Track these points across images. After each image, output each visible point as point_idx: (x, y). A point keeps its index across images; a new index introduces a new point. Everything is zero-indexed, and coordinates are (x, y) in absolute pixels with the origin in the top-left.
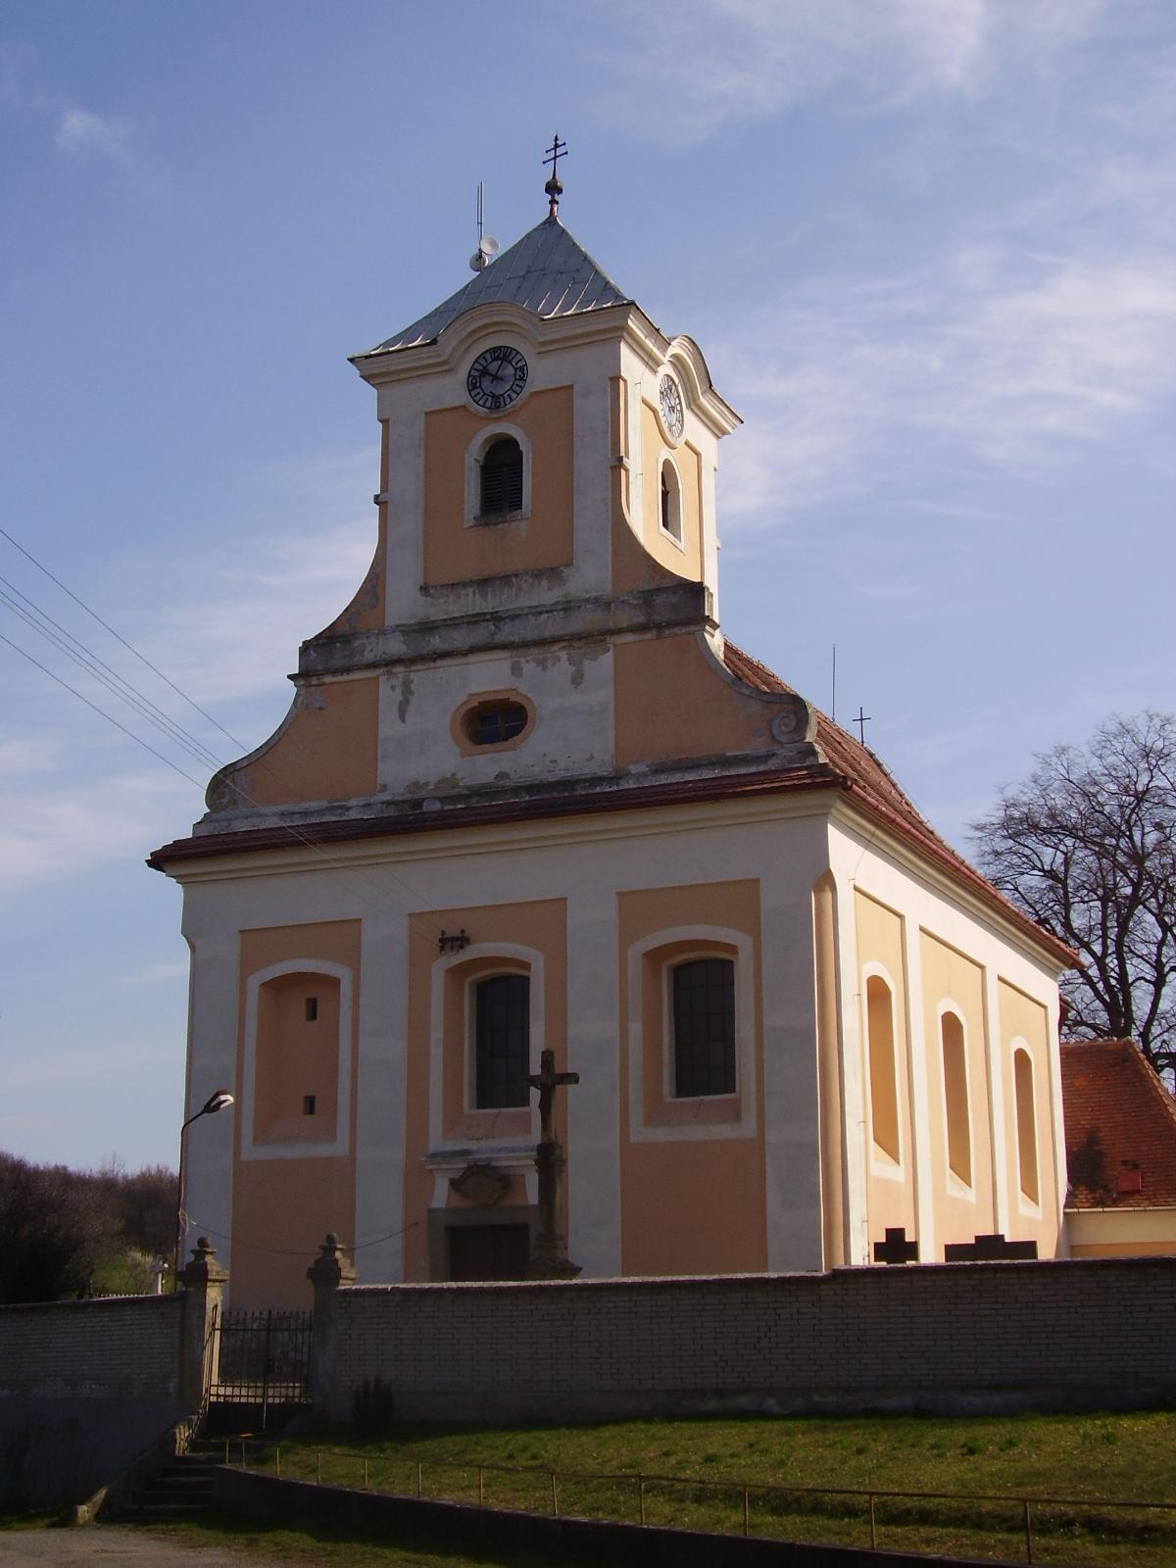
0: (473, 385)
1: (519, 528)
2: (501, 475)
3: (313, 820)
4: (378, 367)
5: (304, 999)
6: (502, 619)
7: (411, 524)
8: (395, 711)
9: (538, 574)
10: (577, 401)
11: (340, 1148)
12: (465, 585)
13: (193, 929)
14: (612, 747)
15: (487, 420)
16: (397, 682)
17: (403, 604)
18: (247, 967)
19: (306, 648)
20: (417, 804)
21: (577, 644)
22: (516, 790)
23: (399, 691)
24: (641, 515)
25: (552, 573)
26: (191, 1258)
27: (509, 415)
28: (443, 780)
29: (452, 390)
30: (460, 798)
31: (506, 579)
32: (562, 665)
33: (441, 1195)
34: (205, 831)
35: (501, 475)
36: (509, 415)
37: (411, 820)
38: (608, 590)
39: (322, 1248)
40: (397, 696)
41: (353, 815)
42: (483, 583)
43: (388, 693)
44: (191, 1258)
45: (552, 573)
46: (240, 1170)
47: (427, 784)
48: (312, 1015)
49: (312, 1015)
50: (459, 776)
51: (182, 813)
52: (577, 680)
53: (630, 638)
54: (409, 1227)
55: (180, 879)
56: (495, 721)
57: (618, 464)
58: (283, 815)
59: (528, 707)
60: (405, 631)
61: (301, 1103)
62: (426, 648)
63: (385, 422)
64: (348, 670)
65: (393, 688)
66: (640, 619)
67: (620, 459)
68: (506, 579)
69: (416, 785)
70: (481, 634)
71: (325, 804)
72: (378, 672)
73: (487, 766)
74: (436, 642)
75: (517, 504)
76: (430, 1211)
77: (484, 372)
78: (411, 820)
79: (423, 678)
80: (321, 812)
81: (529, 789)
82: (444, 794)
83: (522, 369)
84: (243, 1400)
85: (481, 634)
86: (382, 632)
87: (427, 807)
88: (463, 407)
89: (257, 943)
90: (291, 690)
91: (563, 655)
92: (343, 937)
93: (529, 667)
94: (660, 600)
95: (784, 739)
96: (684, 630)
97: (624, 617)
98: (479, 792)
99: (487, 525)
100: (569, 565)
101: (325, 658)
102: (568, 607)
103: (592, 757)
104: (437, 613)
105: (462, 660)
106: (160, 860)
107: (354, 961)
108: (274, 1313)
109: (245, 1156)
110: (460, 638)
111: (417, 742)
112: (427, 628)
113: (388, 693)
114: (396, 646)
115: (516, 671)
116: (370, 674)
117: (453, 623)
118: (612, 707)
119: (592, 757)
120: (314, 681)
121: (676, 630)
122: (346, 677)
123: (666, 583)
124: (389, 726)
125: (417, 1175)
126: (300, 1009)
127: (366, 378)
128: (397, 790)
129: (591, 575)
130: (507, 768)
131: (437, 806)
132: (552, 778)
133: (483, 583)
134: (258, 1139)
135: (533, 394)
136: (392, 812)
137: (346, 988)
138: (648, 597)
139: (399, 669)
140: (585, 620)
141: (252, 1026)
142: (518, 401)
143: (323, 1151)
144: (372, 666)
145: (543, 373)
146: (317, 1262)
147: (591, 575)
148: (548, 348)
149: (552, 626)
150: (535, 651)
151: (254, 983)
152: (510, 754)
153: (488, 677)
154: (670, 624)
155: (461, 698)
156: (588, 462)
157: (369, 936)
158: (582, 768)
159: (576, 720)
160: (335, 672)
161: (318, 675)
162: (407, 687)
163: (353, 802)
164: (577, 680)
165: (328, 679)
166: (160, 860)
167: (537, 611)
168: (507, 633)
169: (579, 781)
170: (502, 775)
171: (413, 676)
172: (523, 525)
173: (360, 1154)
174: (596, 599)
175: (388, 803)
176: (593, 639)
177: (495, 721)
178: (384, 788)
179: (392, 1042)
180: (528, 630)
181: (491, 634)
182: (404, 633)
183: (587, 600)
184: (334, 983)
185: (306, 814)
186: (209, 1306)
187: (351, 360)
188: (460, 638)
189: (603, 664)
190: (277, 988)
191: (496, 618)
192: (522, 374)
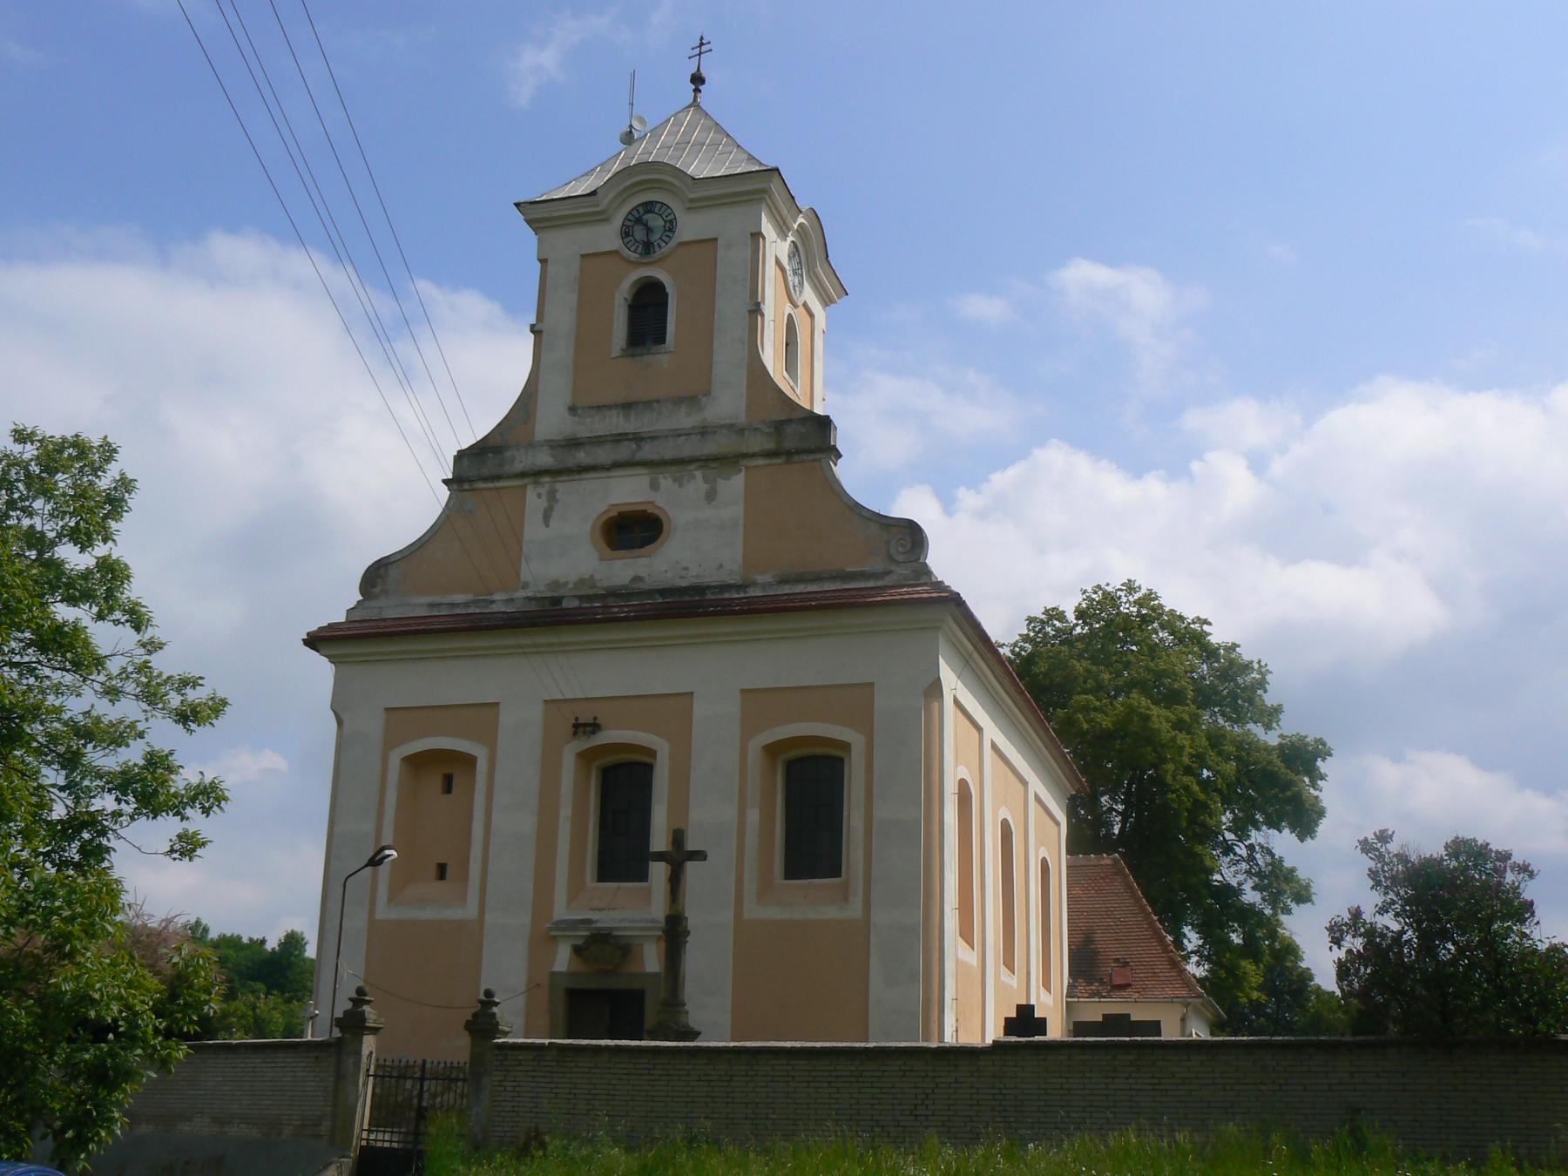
0: (626, 233)
1: (662, 360)
2: (648, 312)
3: (459, 611)
4: (539, 213)
5: (443, 772)
6: (643, 439)
7: (563, 352)
8: (540, 516)
9: (678, 401)
10: (721, 252)
11: (470, 911)
12: (609, 407)
13: (339, 708)
14: (740, 558)
15: (637, 264)
16: (544, 490)
17: (552, 421)
18: (389, 744)
19: (461, 456)
20: (557, 601)
21: (712, 465)
22: (650, 593)
23: (544, 498)
24: (771, 356)
25: (692, 401)
26: (349, 1005)
27: (661, 259)
28: (582, 581)
29: (607, 237)
30: (596, 597)
31: (648, 404)
32: (697, 483)
33: (562, 959)
34: (357, 616)
35: (648, 312)
36: (661, 259)
37: (553, 617)
38: (742, 420)
39: (481, 1002)
40: (543, 503)
41: (495, 608)
42: (627, 406)
43: (534, 500)
44: (349, 1005)
45: (692, 401)
46: (374, 926)
47: (567, 583)
48: (448, 787)
49: (448, 787)
50: (597, 577)
51: (337, 601)
52: (710, 496)
53: (760, 462)
54: (532, 987)
55: (331, 659)
56: (633, 530)
57: (756, 310)
58: (432, 605)
59: (663, 518)
60: (553, 445)
61: (433, 870)
62: (571, 462)
63: (543, 261)
64: (498, 478)
65: (539, 496)
66: (771, 446)
67: (758, 304)
68: (648, 404)
69: (555, 584)
70: (624, 452)
71: (470, 597)
72: (526, 481)
73: (623, 570)
74: (582, 457)
75: (660, 338)
76: (553, 974)
77: (639, 221)
78: (553, 617)
79: (564, 488)
80: (466, 605)
81: (663, 592)
82: (582, 593)
83: (671, 222)
84: (387, 1145)
85: (624, 452)
86: (532, 445)
87: (566, 604)
88: (616, 252)
89: (400, 719)
90: (444, 493)
91: (699, 474)
92: (481, 717)
93: (666, 482)
94: (789, 429)
95: (900, 558)
96: (811, 457)
97: (756, 443)
98: (613, 593)
99: (633, 355)
100: (708, 393)
101: (477, 469)
102: (704, 431)
103: (721, 566)
104: (583, 432)
105: (603, 474)
106: (314, 641)
107: (489, 736)
108: (428, 1066)
109: (379, 916)
110: (603, 455)
111: (559, 545)
112: (573, 444)
113: (534, 500)
114: (544, 459)
115: (655, 486)
116: (518, 482)
117: (597, 441)
118: (741, 522)
119: (721, 566)
120: (466, 486)
121: (804, 457)
122: (498, 484)
123: (795, 416)
124: (534, 530)
125: (545, 936)
126: (436, 782)
127: (530, 222)
128: (539, 589)
129: (727, 403)
130: (642, 572)
131: (576, 603)
132: (684, 583)
133: (627, 406)
134: (392, 898)
135: (681, 244)
136: (533, 607)
137: (482, 766)
138: (779, 426)
139: (546, 479)
140: (720, 444)
141: (392, 797)
142: (665, 249)
143: (453, 914)
144: (522, 475)
145: (690, 226)
146: (475, 1015)
147: (727, 403)
148: (695, 206)
149: (688, 448)
150: (674, 469)
151: (396, 757)
152: (644, 561)
153: (628, 491)
154: (799, 452)
155: (603, 508)
156: (729, 307)
157: (506, 718)
158: (712, 577)
159: (707, 535)
160: (486, 479)
161: (470, 481)
162: (552, 497)
163: (497, 597)
164: (710, 496)
165: (481, 485)
166: (314, 641)
167: (677, 433)
168: (647, 452)
169: (709, 587)
170: (638, 579)
171: (558, 486)
172: (665, 358)
173: (488, 917)
174: (732, 426)
175: (529, 599)
176: (727, 462)
177: (633, 530)
178: (525, 586)
179: (523, 814)
180: (666, 450)
181: (630, 454)
182: (552, 447)
183: (723, 426)
184: (469, 761)
185: (452, 605)
186: (365, 1052)
187: (517, 205)
188: (603, 455)
189: (735, 484)
190: (418, 763)
191: (638, 438)
192: (671, 226)
